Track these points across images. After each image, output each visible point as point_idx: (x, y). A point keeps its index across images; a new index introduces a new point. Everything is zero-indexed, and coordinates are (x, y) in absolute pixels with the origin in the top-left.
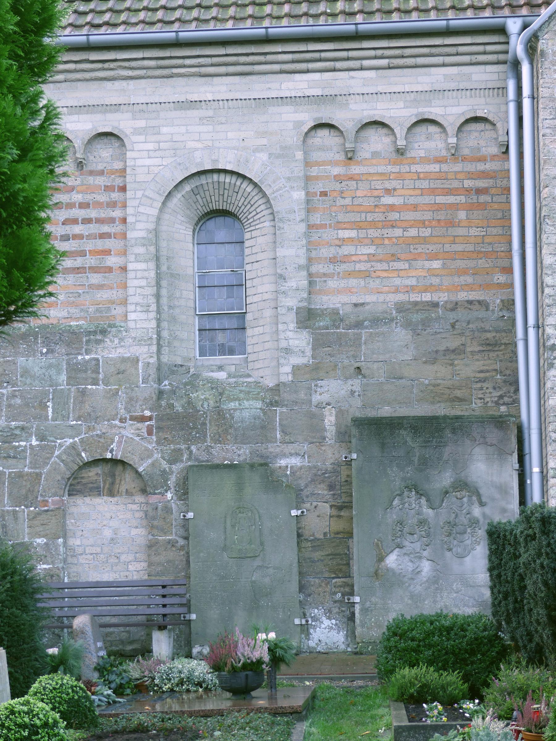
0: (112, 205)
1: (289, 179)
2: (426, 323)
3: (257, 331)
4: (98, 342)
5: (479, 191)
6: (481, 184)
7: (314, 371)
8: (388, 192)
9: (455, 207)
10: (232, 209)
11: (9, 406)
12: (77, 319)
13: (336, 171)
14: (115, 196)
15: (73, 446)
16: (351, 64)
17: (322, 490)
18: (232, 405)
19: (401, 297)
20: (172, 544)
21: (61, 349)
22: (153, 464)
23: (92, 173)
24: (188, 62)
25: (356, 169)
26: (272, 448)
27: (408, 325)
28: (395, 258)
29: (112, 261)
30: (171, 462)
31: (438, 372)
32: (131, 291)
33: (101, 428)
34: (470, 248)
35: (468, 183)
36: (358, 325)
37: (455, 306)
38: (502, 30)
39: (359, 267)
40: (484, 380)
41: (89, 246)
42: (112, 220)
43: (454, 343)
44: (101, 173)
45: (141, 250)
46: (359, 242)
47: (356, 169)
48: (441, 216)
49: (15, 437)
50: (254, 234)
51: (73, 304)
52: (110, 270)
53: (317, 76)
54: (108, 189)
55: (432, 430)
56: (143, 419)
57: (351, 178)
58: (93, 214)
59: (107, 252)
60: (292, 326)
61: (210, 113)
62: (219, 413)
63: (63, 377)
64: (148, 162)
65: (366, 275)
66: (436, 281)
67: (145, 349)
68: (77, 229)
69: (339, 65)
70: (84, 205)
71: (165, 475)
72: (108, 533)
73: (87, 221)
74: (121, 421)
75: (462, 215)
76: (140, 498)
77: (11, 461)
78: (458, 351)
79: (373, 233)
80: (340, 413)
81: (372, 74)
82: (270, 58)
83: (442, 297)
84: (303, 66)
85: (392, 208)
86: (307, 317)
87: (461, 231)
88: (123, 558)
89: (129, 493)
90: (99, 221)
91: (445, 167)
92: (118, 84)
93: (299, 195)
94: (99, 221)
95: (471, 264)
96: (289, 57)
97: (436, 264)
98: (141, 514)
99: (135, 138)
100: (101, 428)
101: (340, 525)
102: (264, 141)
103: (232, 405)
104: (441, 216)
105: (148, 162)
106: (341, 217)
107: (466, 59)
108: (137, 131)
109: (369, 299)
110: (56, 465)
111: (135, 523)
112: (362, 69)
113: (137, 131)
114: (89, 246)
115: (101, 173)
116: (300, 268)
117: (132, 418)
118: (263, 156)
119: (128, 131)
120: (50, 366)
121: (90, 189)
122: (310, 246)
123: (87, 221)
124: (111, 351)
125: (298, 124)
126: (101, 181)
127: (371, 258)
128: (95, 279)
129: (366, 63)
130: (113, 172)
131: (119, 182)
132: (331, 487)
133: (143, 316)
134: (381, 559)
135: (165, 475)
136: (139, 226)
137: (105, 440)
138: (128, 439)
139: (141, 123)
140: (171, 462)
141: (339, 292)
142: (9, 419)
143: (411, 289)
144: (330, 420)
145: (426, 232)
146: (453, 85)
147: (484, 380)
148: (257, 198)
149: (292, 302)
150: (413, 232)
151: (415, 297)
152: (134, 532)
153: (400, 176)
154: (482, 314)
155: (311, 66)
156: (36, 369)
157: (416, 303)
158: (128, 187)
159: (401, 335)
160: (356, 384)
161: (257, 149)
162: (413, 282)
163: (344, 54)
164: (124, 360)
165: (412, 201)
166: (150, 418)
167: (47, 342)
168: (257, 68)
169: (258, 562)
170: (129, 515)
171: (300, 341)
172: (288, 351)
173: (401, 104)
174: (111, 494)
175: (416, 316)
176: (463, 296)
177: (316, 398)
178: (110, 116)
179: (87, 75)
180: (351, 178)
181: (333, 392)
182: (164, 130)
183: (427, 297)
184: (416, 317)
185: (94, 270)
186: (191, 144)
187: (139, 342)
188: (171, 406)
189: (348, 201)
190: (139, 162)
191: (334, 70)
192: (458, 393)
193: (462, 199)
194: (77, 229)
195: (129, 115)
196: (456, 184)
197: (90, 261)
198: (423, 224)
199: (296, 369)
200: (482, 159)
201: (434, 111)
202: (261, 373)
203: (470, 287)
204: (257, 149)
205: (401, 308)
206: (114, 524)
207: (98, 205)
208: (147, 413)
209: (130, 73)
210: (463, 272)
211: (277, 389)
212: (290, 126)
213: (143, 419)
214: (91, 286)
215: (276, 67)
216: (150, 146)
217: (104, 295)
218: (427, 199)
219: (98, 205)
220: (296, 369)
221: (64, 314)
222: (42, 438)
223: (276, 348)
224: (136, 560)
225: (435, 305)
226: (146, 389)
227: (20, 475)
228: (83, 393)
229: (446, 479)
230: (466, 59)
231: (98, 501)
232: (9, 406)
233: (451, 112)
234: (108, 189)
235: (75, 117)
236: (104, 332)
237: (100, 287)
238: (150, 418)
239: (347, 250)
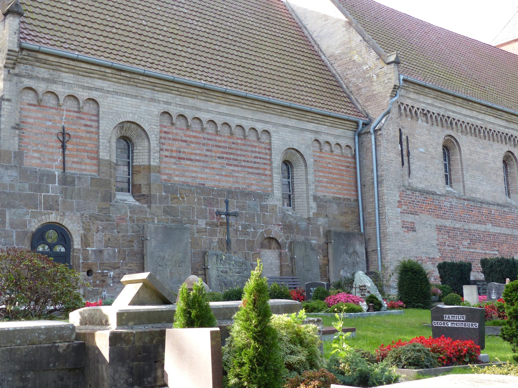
0: (266, 154)
1: (310, 155)
2: (340, 203)
3: (299, 200)
4: (267, 199)
5: (348, 167)
6: (348, 165)
7: (317, 215)
8: (329, 163)
9: (343, 170)
10: (291, 161)
11: (245, 217)
12: (259, 190)
13: (318, 154)
14: (267, 151)
15: (262, 232)
16: (323, 123)
17: (320, 251)
18: (300, 223)
19: (333, 195)
20: (288, 265)
21: (258, 200)
22: (282, 240)
23: (261, 142)
24: (288, 113)
25: (322, 155)
26: (310, 237)
27: (336, 204)
28: (331, 183)
29: (268, 172)
30: (287, 239)
31: (342, 219)
32: (274, 183)
33: (269, 227)
34: (347, 183)
35: (346, 164)
36: (326, 202)
37: (344, 199)
38: (357, 123)
39: (325, 184)
40: (352, 222)
41: (261, 166)
42: (266, 159)
43: (346, 211)
44: (263, 143)
45: (276, 170)
46: (324, 177)
47: (322, 155)
48: (340, 172)
49: (247, 228)
50: (298, 170)
51: (258, 185)
52: (266, 175)
53: (314, 124)
54: (265, 148)
55: (349, 236)
56: (279, 225)
57: (321, 157)
58: (262, 156)
59: (265, 169)
60: (312, 200)
61: (291, 130)
62: (297, 225)
63: (259, 209)
64: (276, 142)
65: (326, 187)
66: (340, 191)
67: (278, 203)
68: (258, 160)
69: (321, 123)
70: (259, 153)
71: (285, 243)
72: (269, 261)
73: (260, 158)
74: (274, 225)
75: (344, 173)
76: (277, 251)
77: (247, 236)
78: (346, 213)
79: (327, 175)
80: (324, 228)
81: (326, 127)
82: (307, 117)
83: (341, 196)
84: (313, 121)
85: (330, 168)
86: (315, 198)
87: (344, 178)
88: (274, 269)
89: (274, 249)
90: (263, 159)
91: (341, 158)
92: (269, 115)
93: (312, 160)
94: (263, 159)
95: (347, 187)
96: (311, 117)
97: (340, 186)
98: (277, 256)
99: (273, 134)
100: (269, 227)
101: (325, 262)
102: (303, 142)
103: (300, 223)
104: (340, 172)
105: (276, 142)
106: (320, 169)
107: (346, 128)
108: (274, 132)
109: (327, 194)
110: (258, 239)
111: (276, 258)
112: (325, 125)
113: (274, 132)
114: (261, 166)
115: (263, 143)
116: (313, 183)
117: (277, 225)
118: (304, 146)
119: (271, 131)
120: (255, 205)
121: (260, 148)
122: (315, 176)
123: (260, 158)
124: (270, 202)
125: (311, 138)
126: (263, 145)
127: (327, 182)
128: (263, 177)
129: (327, 124)
130: (266, 143)
131: (268, 147)
132: (322, 250)
133: (278, 192)
134: (339, 272)
135: (285, 243)
136: (276, 162)
137: (269, 231)
138: (276, 231)
139: (274, 129)
140: (287, 239)
141: (320, 191)
142: (246, 221)
143: (335, 193)
144: (321, 230)
145: (338, 177)
146: (343, 135)
147: (352, 222)
148: (301, 160)
149: (311, 193)
150: (335, 176)
151: (336, 196)
152: (276, 261)
153: (331, 159)
154: (349, 202)
155: (315, 121)
156: (252, 205)
157: (336, 197)
158: (272, 149)
159: (335, 206)
160: (327, 219)
161: (302, 144)
162: (335, 191)
163: (322, 120)
164: (274, 205)
165: (335, 167)
166: (281, 225)
167: (254, 197)
168: (303, 119)
169: (311, 272)
170: (274, 256)
171: (313, 205)
172: (311, 207)
173: (333, 138)
174: (270, 249)
175: (337, 200)
176: (346, 197)
177: (318, 223)
178: (267, 125)
179: (262, 110)
180: (321, 157)
181: (321, 221)
182: (281, 133)
183: (338, 196)
184: (338, 201)
185: (263, 174)
186: (287, 139)
187: (278, 200)
188: (286, 222)
189: (320, 164)
190: (275, 142)
191: (319, 124)
192: (347, 225)
193: (344, 168)
194: (258, 160)
195: (271, 126)
196: (343, 164)
197: (262, 172)
198: (337, 174)
199: (314, 213)
200: (347, 157)
201: (340, 142)
202: (301, 214)
203: (344, 194)
204: (302, 144)
205: (335, 198)
206: (271, 258)
207: (263, 153)
208: (280, 223)
209: (272, 112)
210: (345, 190)
211: (309, 219)
212: (309, 138)
213: (279, 225)
214: (262, 180)
215: (307, 120)
216: (277, 137)
217: (266, 183)
218: (337, 167)
219: (263, 153)
220: (314, 213)
221: (255, 188)
222: (254, 229)
223: (305, 208)
224: (277, 270)
225: (340, 198)
226: (279, 216)
227: (249, 241)
228: (264, 215)
229: (351, 250)
230: (346, 128)
231: (266, 250)
232: (245, 217)
233: (343, 142)
234: (265, 148)
235: (258, 123)
236: (268, 196)
237: (265, 180)
238: (281, 225)
239: (321, 179)
